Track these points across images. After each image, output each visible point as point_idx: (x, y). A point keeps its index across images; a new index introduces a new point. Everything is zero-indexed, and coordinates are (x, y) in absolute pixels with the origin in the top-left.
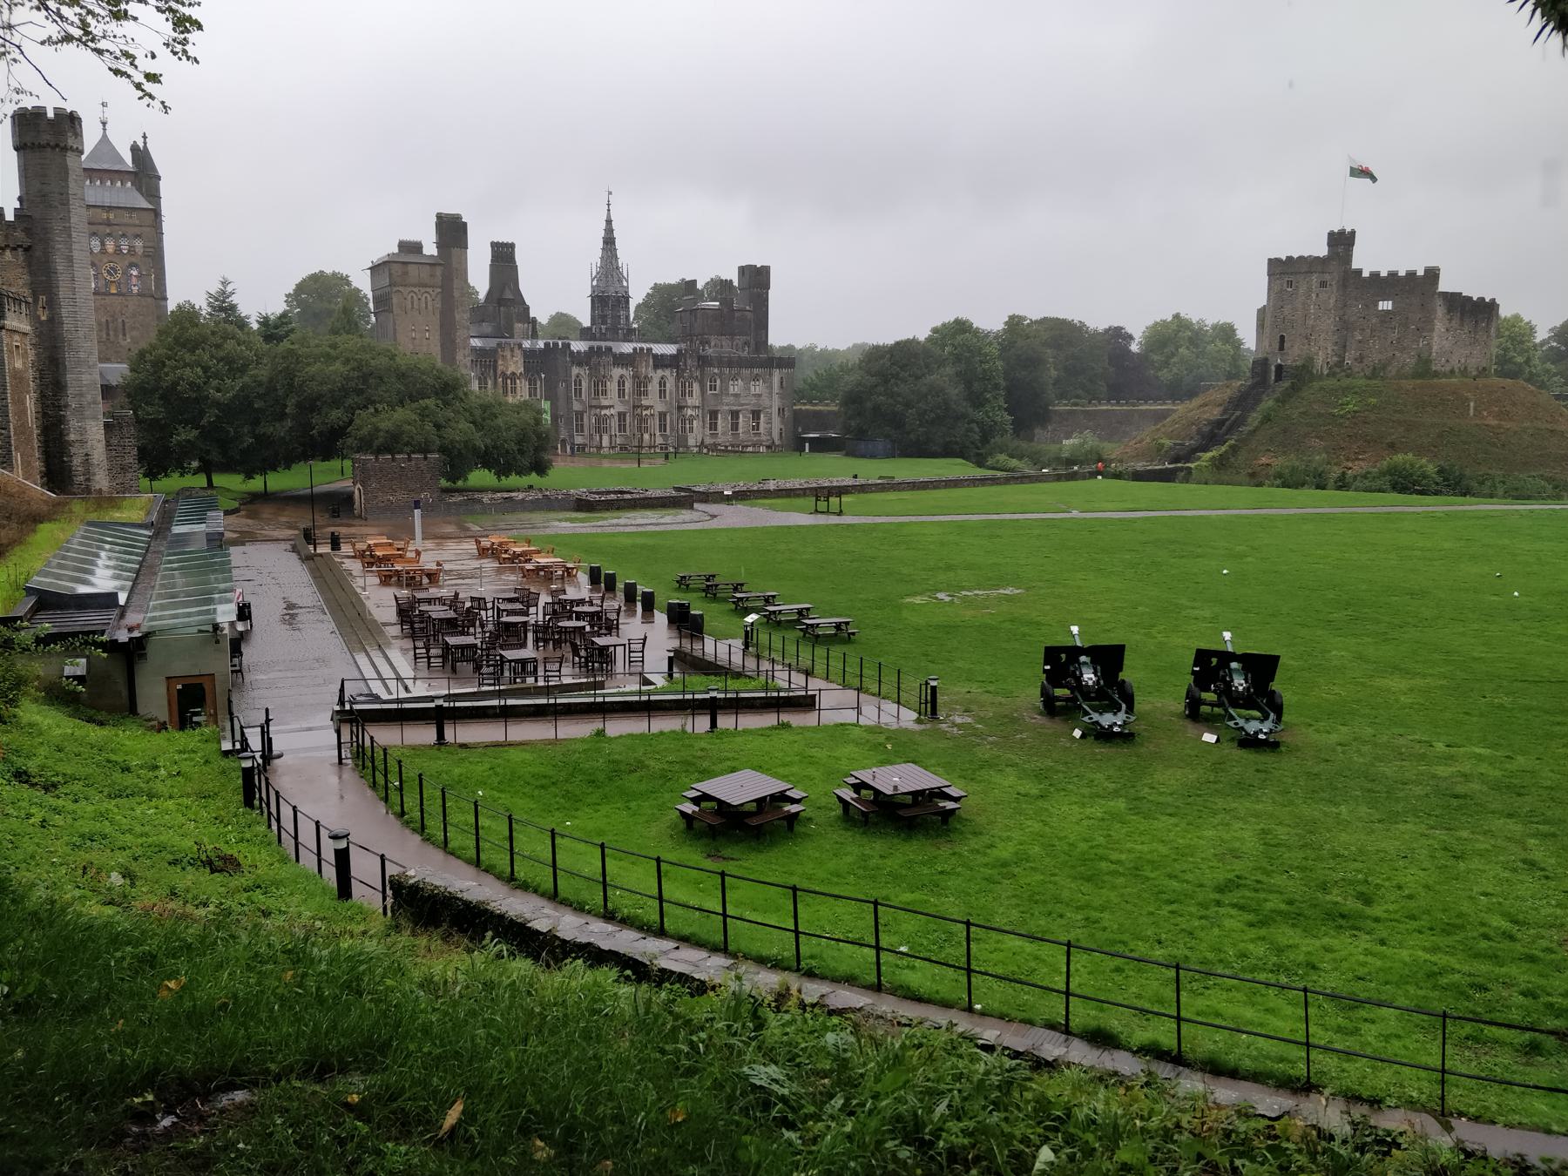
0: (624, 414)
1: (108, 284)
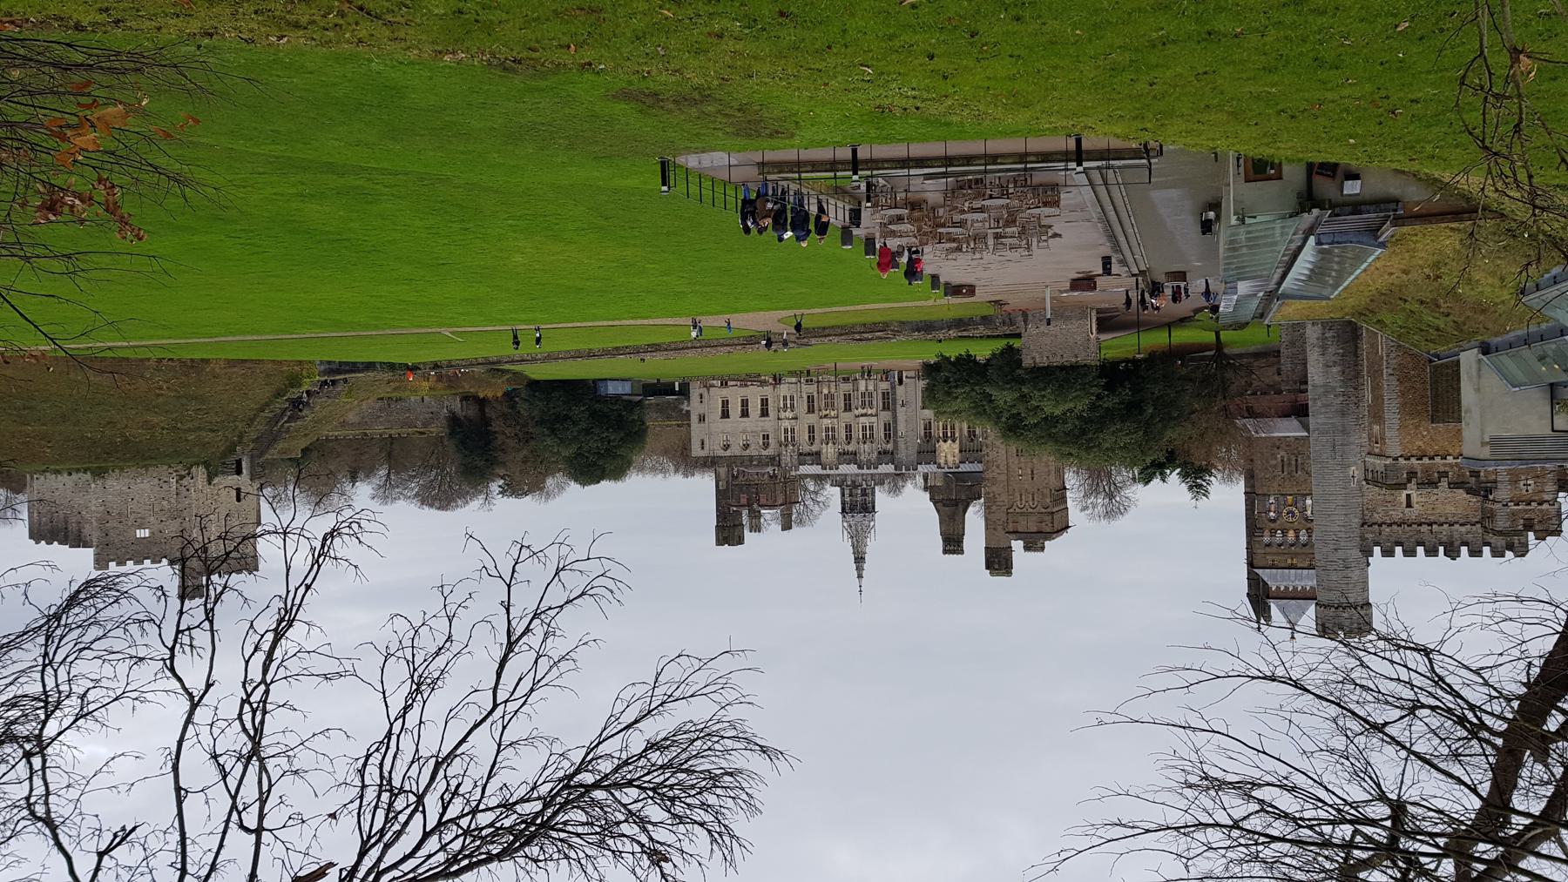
0: (845, 410)
1: (1295, 504)
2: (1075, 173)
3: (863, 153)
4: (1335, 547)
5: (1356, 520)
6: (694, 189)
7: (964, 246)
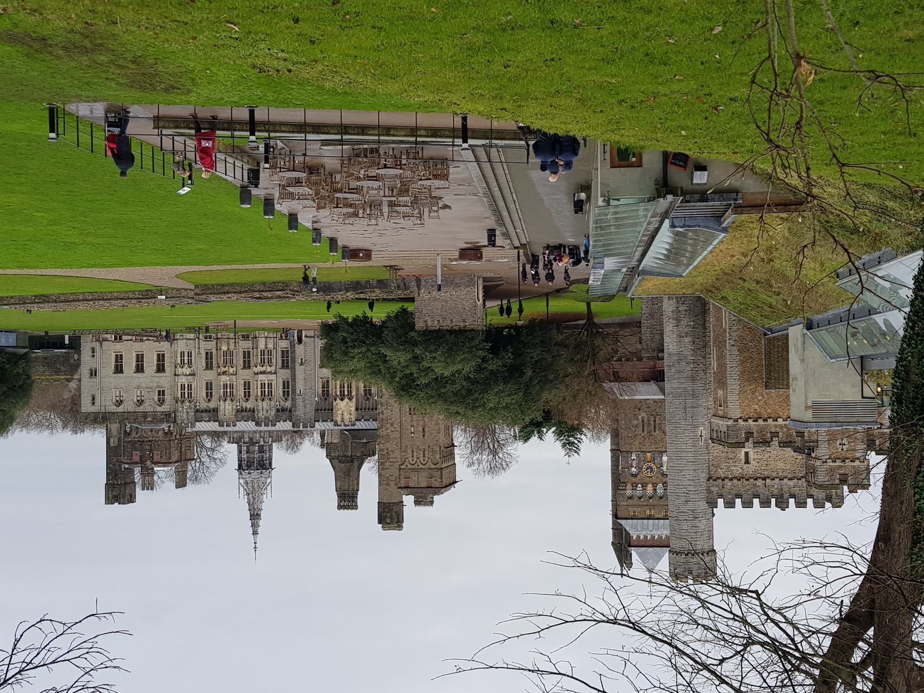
0: (244, 368)
1: (653, 460)
2: (462, 151)
3: (260, 115)
4: (686, 499)
5: (704, 475)
6: (85, 138)
7: (361, 212)
